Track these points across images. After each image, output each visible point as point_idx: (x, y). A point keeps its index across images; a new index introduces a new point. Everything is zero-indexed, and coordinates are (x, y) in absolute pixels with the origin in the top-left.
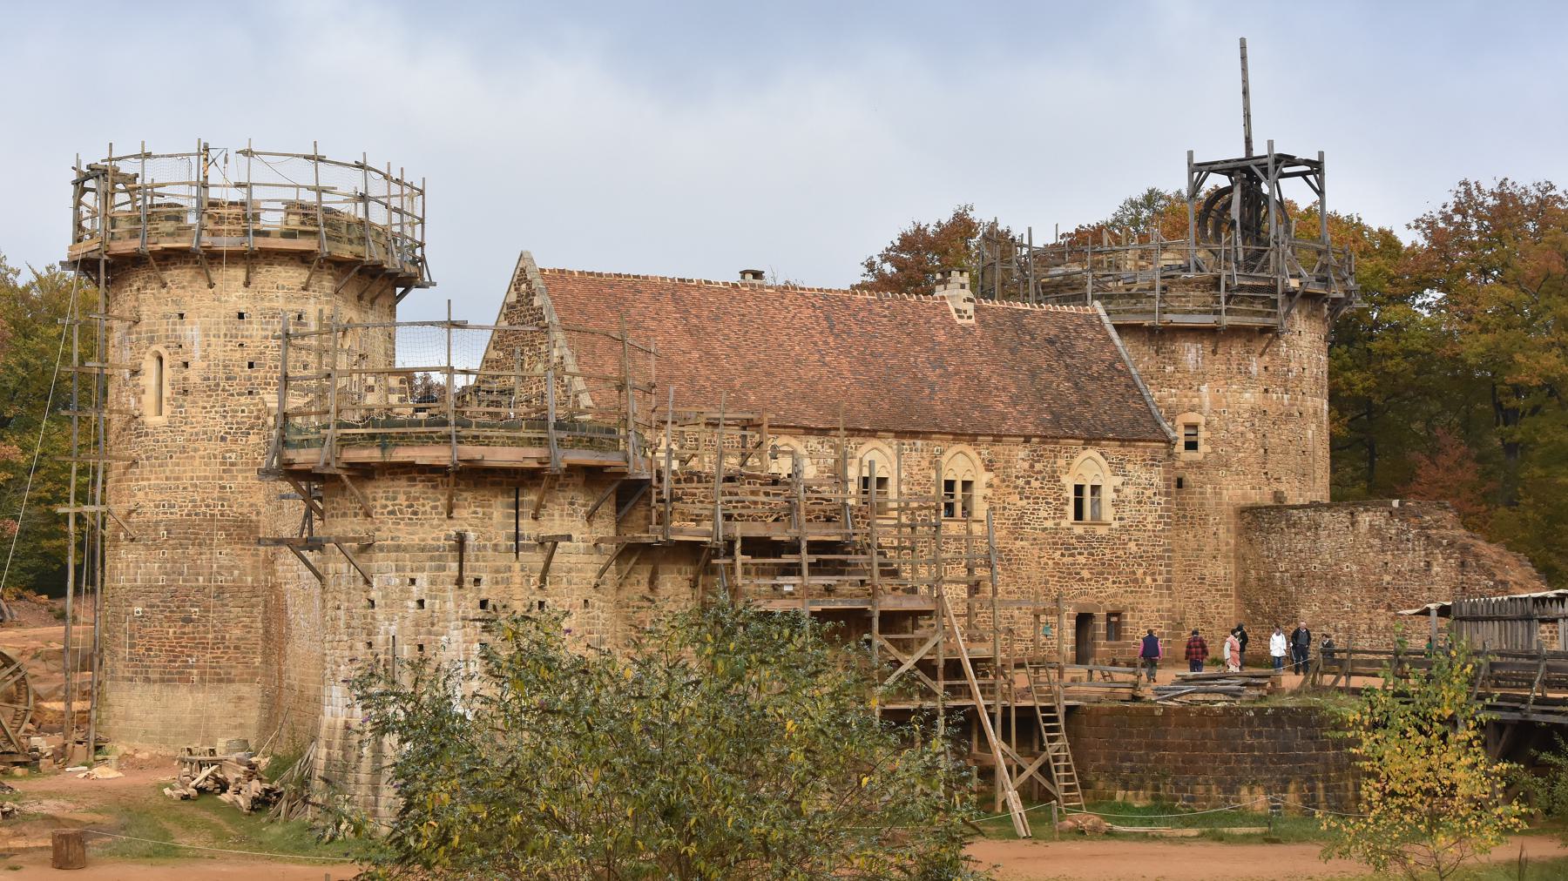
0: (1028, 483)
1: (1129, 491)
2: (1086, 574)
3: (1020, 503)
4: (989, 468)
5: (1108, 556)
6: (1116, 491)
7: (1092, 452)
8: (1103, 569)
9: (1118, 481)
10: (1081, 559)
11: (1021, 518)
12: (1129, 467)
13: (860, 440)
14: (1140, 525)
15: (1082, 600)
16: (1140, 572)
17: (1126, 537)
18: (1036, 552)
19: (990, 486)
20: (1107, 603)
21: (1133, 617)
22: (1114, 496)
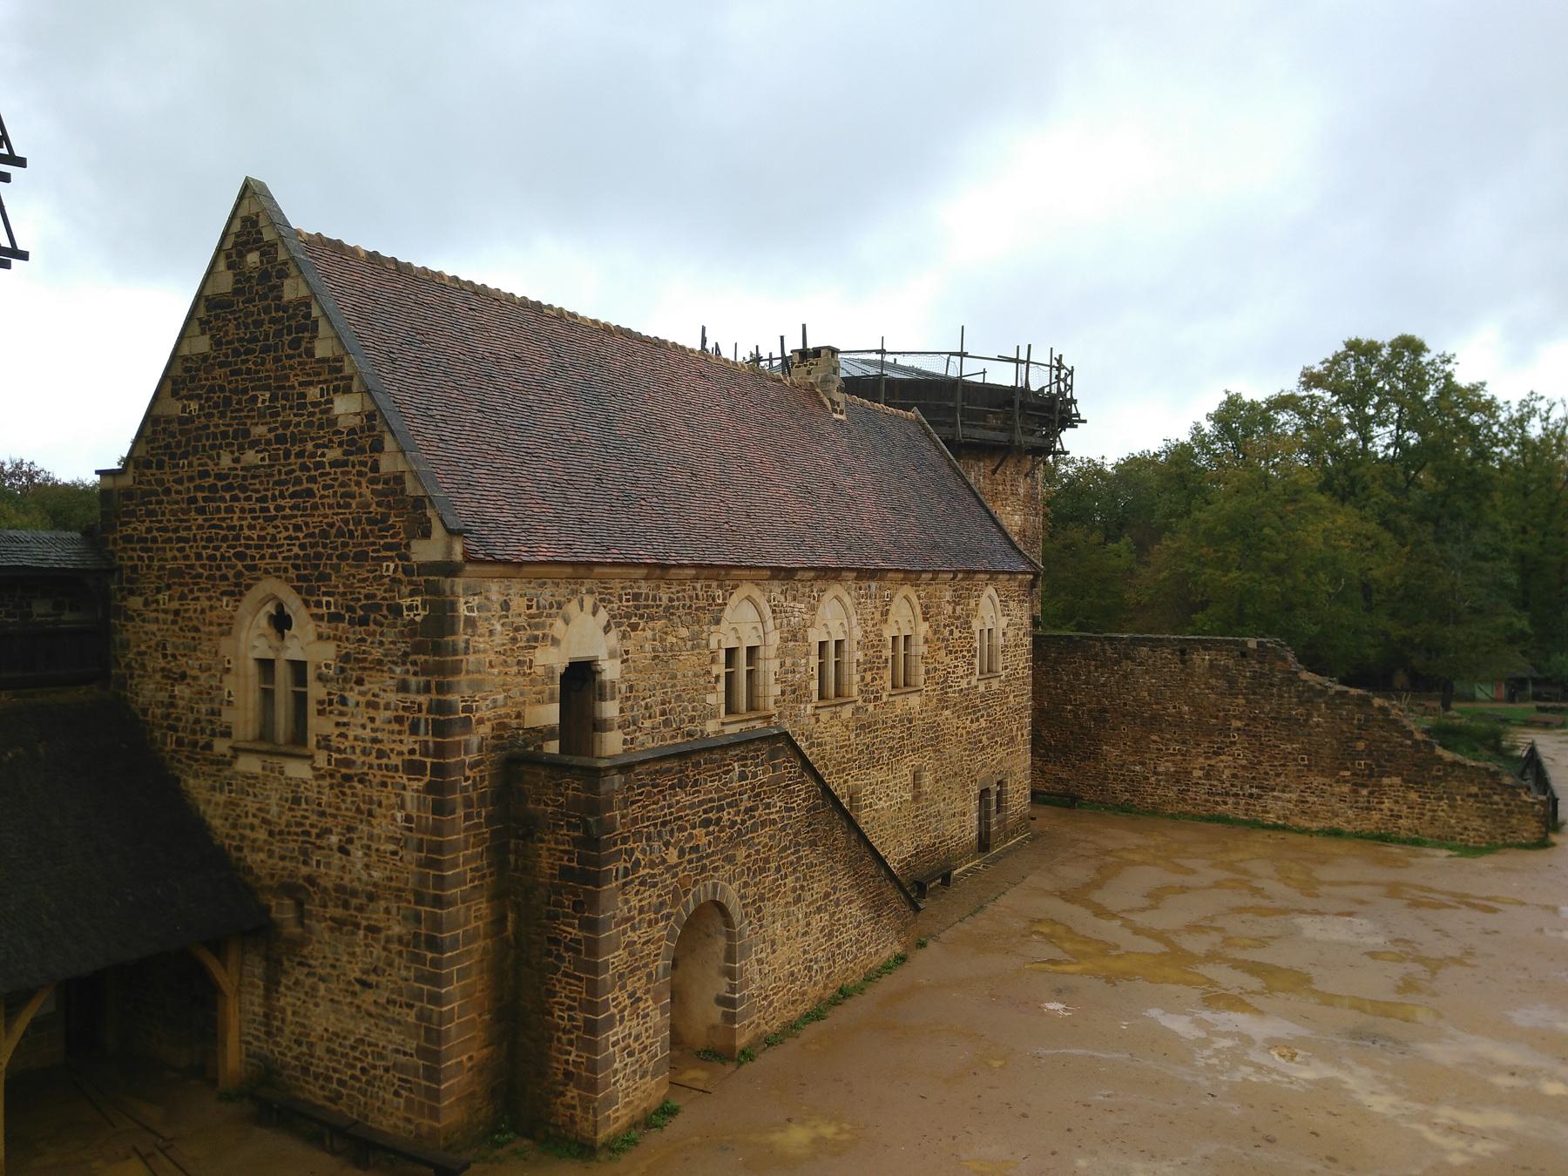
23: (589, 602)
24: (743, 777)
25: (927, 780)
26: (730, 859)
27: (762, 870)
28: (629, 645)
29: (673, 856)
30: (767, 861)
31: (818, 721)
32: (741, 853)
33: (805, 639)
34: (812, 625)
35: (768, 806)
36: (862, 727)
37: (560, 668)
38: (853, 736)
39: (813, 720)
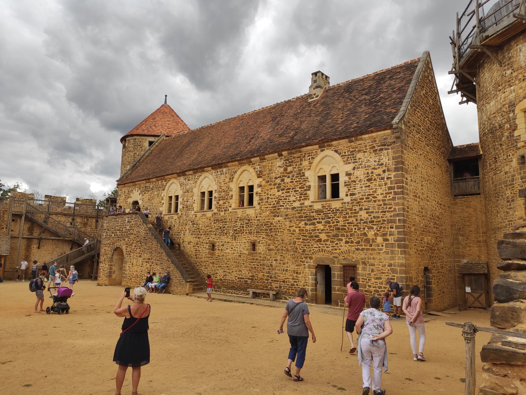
0: (283, 180)
1: (360, 174)
2: (323, 236)
3: (277, 194)
4: (259, 177)
5: (341, 223)
6: (348, 174)
7: (329, 152)
8: (338, 233)
9: (349, 168)
10: (320, 226)
11: (278, 203)
12: (359, 155)
13: (200, 174)
14: (370, 197)
15: (320, 255)
16: (371, 234)
17: (357, 208)
18: (287, 223)
19: (260, 186)
20: (341, 257)
21: (364, 269)
22: (347, 178)
23: (137, 189)
24: (128, 222)
25: (261, 248)
26: (124, 240)
27: (131, 245)
28: (143, 197)
29: (113, 235)
30: (133, 243)
31: (196, 216)
32: (127, 239)
33: (192, 192)
34: (195, 187)
35: (133, 230)
36: (217, 220)
37: (131, 202)
38: (212, 223)
39: (194, 216)
